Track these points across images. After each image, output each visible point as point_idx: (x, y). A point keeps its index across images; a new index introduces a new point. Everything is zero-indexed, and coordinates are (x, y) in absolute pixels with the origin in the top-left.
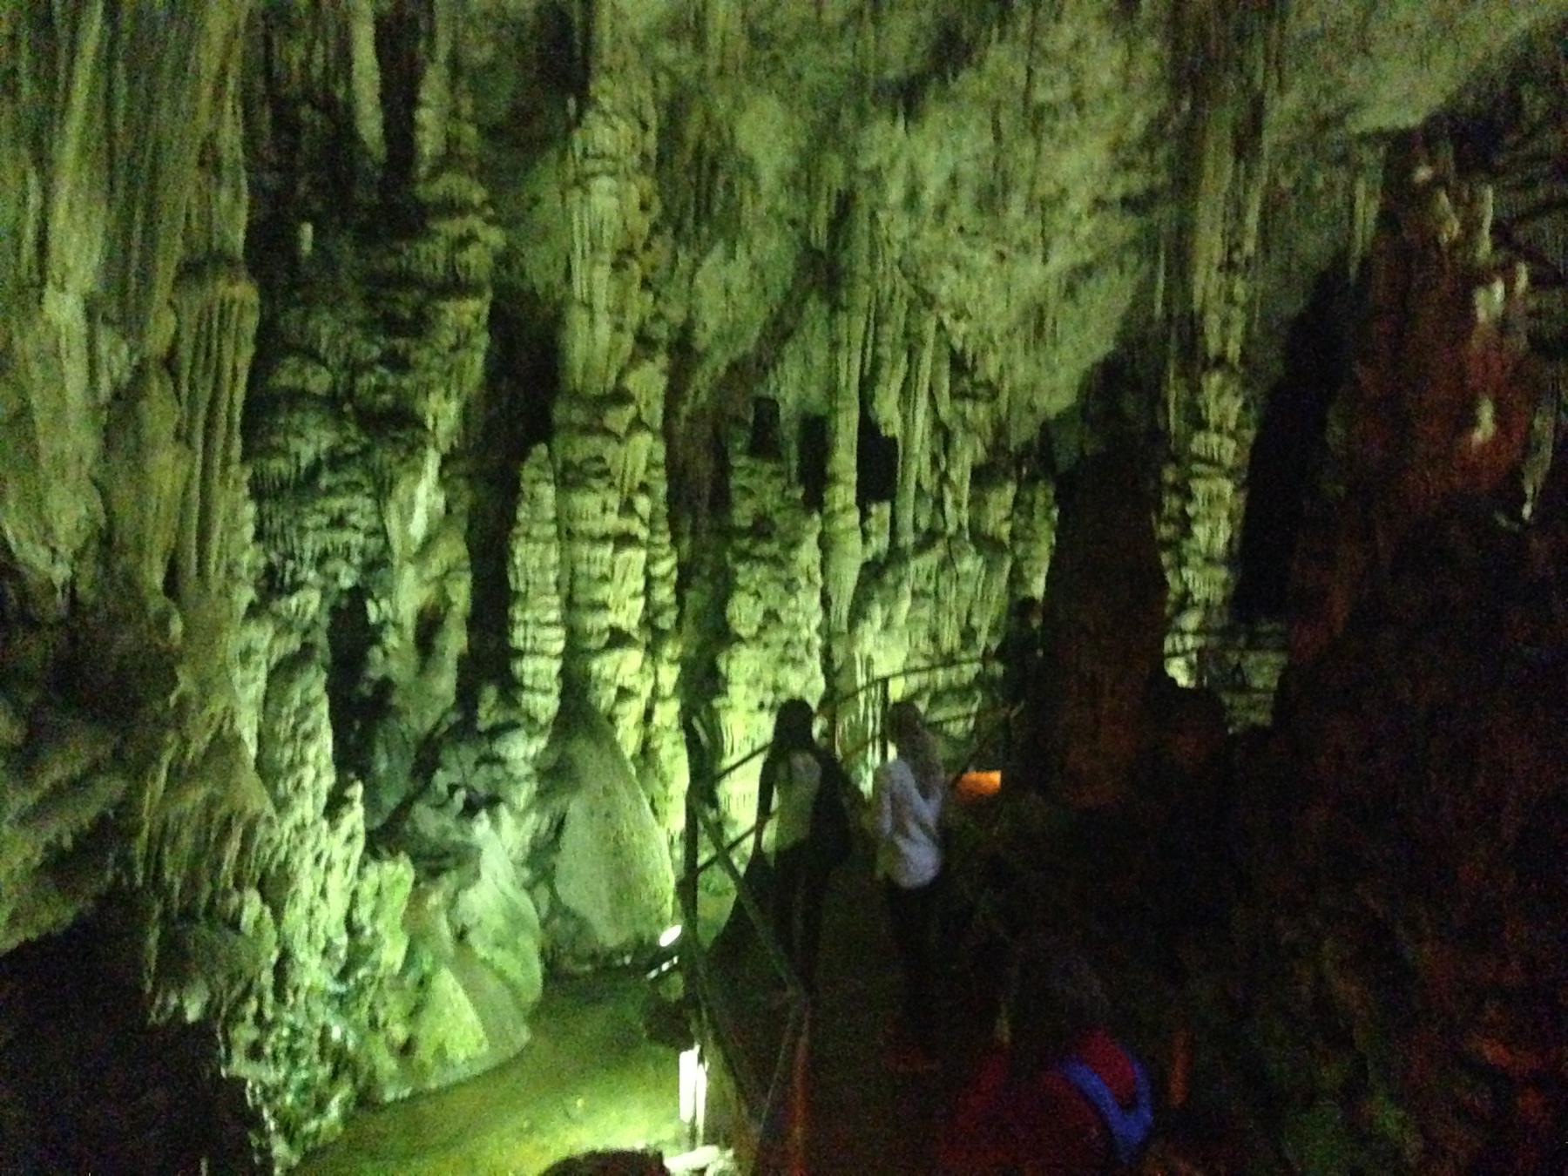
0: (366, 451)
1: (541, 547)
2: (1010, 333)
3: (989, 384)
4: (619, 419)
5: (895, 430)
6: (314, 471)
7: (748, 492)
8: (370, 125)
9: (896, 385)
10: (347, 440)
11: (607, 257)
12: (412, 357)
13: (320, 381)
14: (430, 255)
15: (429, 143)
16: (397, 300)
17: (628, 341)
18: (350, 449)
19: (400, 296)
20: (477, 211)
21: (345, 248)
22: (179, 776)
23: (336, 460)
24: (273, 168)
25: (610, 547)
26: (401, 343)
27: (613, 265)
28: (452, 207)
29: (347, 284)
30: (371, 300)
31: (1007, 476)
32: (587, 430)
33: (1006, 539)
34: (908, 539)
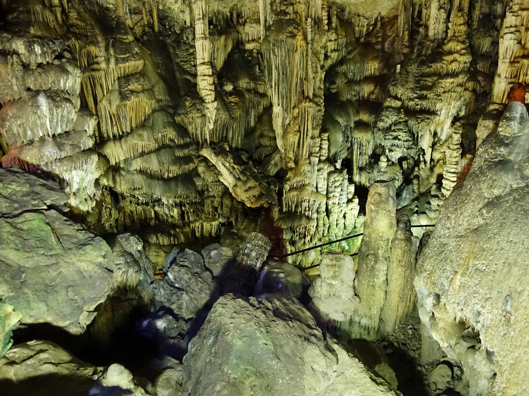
0: (406, 122)
1: (451, 151)
6: (391, 125)
10: (400, 118)
11: (507, 61)
12: (428, 96)
13: (399, 103)
16: (426, 81)
18: (401, 120)
19: (428, 79)
20: (457, 52)
21: (413, 68)
22: (292, 189)
23: (396, 124)
24: (408, 47)
26: (425, 92)
27: (510, 62)
28: (450, 53)
29: (411, 79)
30: (418, 82)
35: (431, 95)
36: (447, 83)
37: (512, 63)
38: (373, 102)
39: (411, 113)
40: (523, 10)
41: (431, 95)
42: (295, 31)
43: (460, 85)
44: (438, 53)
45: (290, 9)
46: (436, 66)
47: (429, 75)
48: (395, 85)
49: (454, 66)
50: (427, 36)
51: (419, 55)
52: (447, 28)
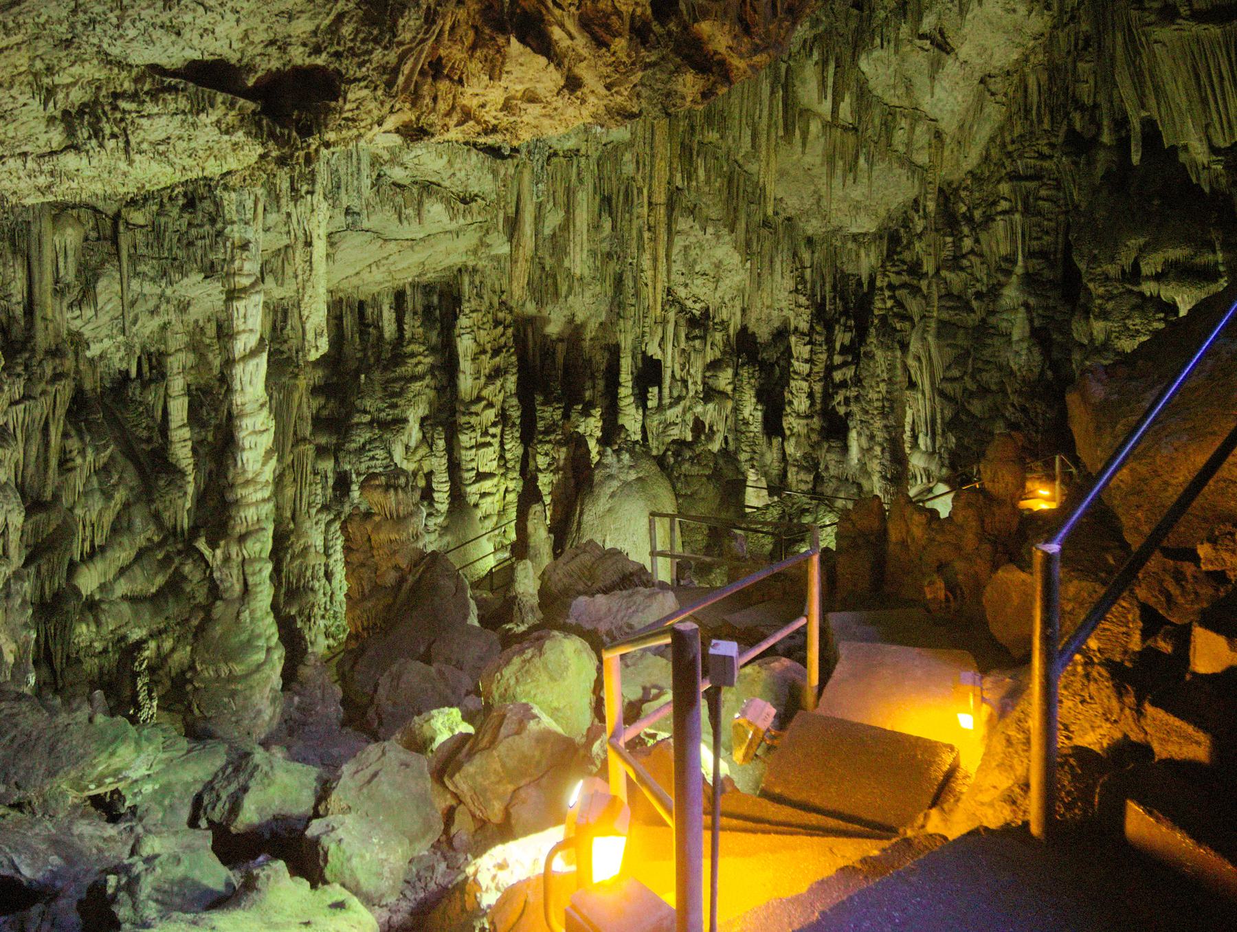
2: (733, 299)
3: (723, 322)
4: (478, 408)
5: (658, 355)
7: (543, 419)
8: (389, 329)
9: (657, 339)
14: (406, 369)
15: (408, 335)
17: (483, 380)
20: (421, 354)
21: (377, 375)
25: (474, 450)
26: (395, 400)
28: (413, 355)
30: (385, 389)
31: (728, 366)
32: (464, 414)
33: (730, 393)
34: (667, 401)
35: (401, 402)
36: (416, 386)
37: (473, 360)
38: (327, 419)
39: (385, 425)
40: (472, 312)
41: (401, 402)
42: (296, 371)
43: (427, 386)
44: (398, 358)
45: (285, 348)
46: (401, 371)
47: (395, 380)
48: (362, 398)
49: (420, 369)
50: (381, 336)
51: (378, 360)
52: (400, 329)
